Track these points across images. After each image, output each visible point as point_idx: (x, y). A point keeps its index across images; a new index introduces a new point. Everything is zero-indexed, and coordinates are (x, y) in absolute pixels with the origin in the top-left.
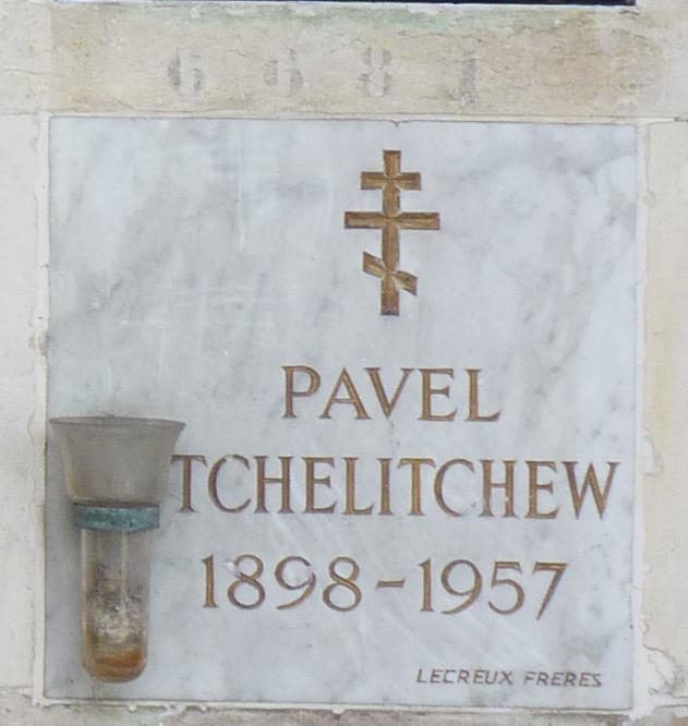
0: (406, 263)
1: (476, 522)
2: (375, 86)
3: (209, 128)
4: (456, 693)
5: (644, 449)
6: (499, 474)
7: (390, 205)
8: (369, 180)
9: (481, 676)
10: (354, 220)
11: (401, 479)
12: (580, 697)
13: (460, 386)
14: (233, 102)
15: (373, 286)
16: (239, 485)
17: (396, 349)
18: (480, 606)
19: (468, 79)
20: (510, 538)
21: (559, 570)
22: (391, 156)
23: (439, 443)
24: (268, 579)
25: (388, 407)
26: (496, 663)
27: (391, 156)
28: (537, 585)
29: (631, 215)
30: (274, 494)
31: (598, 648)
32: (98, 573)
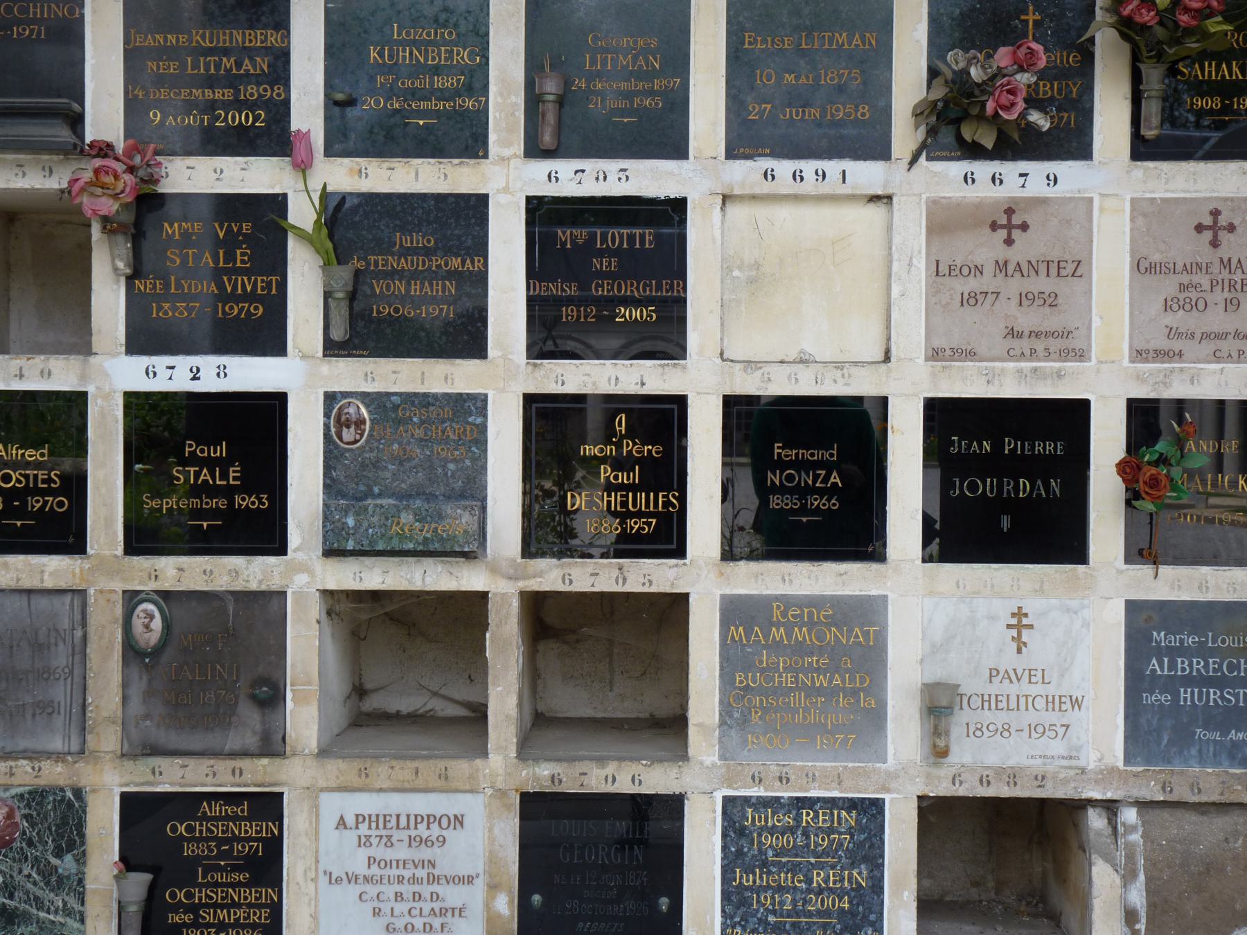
0: (1024, 639)
1: (1044, 713)
2: (1015, 588)
3: (968, 600)
4: (1039, 762)
5: (1092, 692)
6: (1050, 699)
7: (1019, 622)
8: (1013, 615)
9: (1045, 757)
10: (1009, 626)
11: (1022, 700)
12: (1074, 763)
13: (1039, 674)
14: (974, 593)
15: (1014, 645)
16: (976, 702)
17: (1021, 663)
18: (1045, 737)
19: (1041, 586)
20: (1053, 717)
21: (1068, 726)
22: (1020, 608)
23: (1033, 690)
24: (984, 729)
25: (1019, 680)
26: (1049, 753)
27: (1020, 608)
28: (1061, 731)
29: (1088, 625)
30: (986, 704)
31: (1079, 749)
32: (936, 727)
